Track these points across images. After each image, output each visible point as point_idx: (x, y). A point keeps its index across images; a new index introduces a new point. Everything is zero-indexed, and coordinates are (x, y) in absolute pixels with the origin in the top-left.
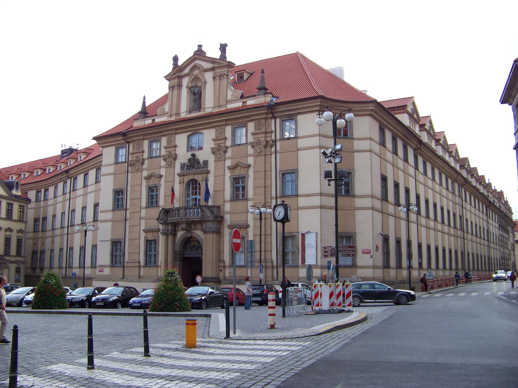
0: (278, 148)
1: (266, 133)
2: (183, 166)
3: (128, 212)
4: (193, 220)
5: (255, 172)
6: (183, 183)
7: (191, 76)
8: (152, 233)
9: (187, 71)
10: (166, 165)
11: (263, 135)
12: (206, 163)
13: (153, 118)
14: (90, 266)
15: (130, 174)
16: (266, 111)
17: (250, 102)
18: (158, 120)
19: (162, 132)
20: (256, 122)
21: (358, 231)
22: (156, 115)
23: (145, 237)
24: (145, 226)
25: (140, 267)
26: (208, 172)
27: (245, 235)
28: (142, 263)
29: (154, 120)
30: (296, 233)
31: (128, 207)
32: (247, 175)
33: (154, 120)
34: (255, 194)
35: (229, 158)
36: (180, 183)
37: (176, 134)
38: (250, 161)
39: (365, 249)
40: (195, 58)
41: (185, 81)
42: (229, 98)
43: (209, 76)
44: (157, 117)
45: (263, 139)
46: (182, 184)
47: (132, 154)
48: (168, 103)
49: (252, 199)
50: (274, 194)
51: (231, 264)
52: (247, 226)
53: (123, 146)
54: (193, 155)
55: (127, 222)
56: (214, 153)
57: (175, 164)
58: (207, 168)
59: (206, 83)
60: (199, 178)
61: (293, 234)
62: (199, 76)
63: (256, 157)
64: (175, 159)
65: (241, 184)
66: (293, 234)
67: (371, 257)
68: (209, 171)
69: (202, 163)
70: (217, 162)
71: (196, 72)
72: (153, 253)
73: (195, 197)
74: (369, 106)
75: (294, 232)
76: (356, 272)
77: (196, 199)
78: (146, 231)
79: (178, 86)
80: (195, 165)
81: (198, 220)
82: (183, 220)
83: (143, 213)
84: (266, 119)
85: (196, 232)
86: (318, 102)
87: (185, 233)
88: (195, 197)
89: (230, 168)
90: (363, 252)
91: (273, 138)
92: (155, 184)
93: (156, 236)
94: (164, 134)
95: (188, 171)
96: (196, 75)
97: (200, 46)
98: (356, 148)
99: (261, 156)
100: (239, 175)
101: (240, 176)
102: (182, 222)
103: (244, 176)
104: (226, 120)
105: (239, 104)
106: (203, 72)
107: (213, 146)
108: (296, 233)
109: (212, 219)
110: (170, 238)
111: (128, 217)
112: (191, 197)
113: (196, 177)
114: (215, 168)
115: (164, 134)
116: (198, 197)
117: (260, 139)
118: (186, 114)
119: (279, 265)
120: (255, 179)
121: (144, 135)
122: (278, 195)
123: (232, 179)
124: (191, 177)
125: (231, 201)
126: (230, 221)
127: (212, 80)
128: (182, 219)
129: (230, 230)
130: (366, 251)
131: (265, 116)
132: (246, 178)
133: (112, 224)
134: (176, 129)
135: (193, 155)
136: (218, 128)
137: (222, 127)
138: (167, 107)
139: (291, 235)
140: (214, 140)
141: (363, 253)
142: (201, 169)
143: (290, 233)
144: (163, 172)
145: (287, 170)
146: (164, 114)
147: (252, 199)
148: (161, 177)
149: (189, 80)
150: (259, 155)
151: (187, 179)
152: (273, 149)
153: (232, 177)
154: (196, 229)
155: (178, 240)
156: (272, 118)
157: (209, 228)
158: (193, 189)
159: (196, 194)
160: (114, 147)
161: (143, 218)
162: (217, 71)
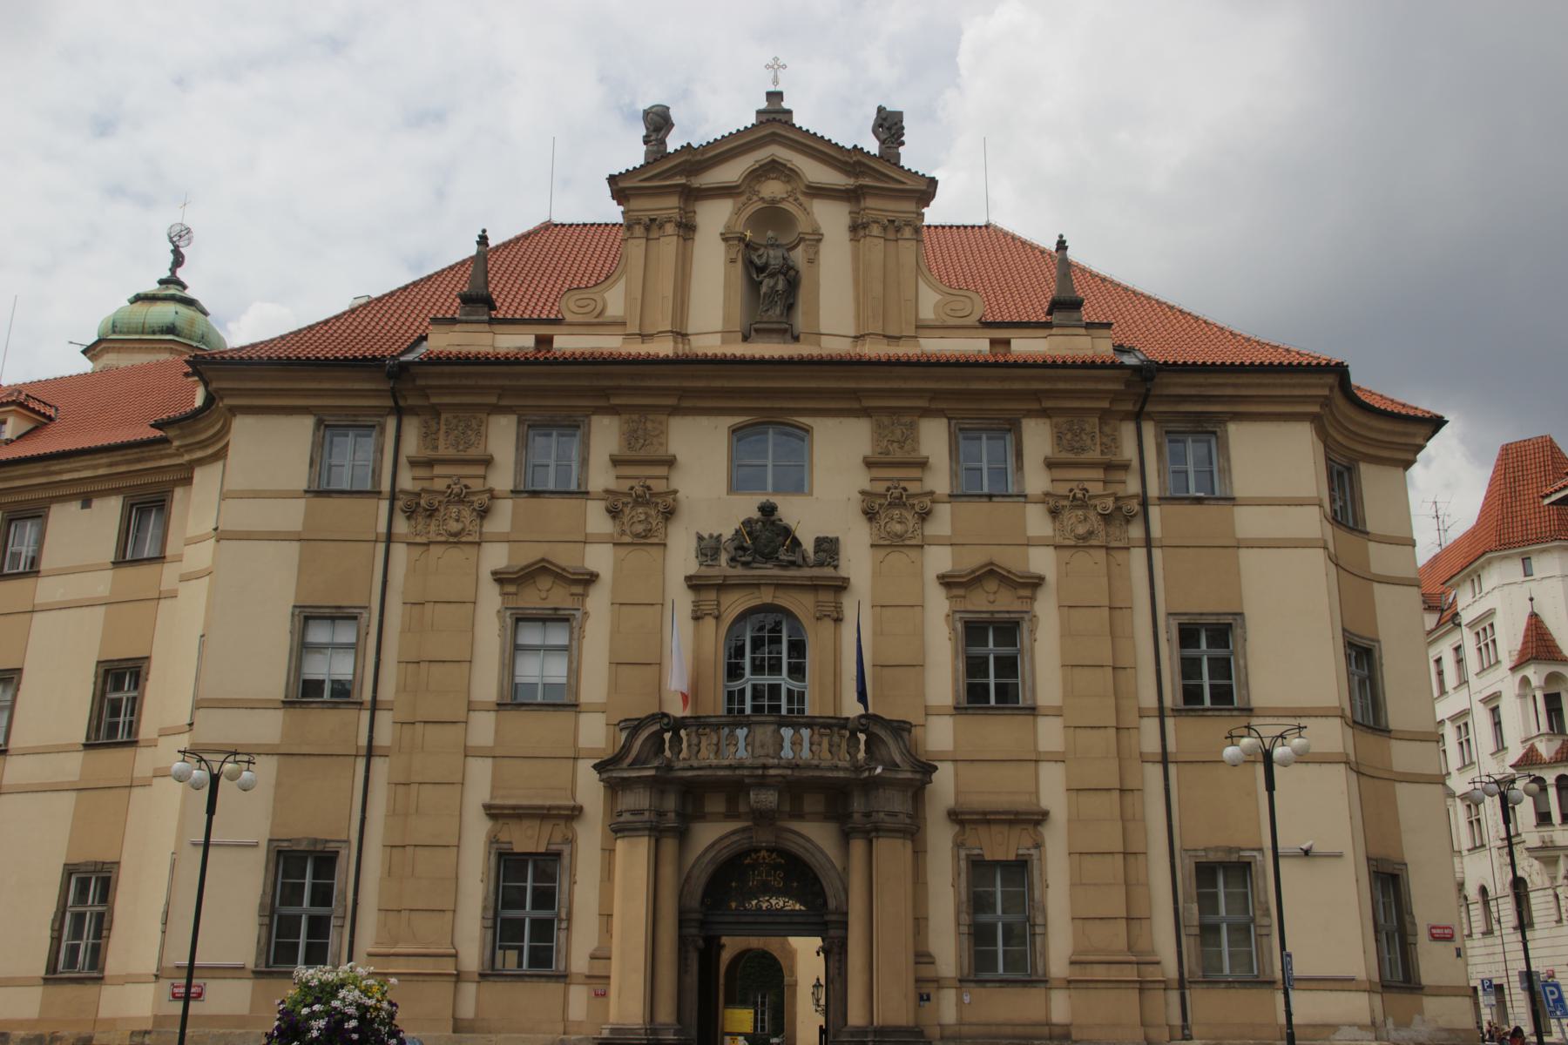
0: (1156, 531)
1: (1109, 467)
2: (708, 549)
3: (384, 718)
4: (817, 773)
5: (1067, 607)
6: (717, 618)
7: (743, 199)
8: (536, 823)
9: (730, 173)
10: (623, 533)
11: (1099, 474)
12: (828, 548)
13: (544, 330)
14: (42, 973)
15: (400, 552)
16: (1120, 387)
17: (1025, 346)
18: (566, 343)
19: (605, 393)
20: (1061, 420)
21: (1408, 858)
22: (557, 322)
23: (493, 840)
24: (494, 788)
25: (458, 977)
26: (841, 586)
27: (1033, 851)
28: (472, 956)
29: (544, 342)
30: (1253, 850)
31: (387, 692)
32: (1026, 617)
33: (544, 342)
34: (1068, 690)
35: (939, 542)
36: (697, 618)
37: (675, 411)
38: (1042, 562)
39: (1434, 923)
40: (774, 134)
41: (714, 217)
42: (927, 313)
43: (831, 219)
44: (564, 329)
45: (1096, 488)
46: (709, 623)
47: (414, 463)
48: (623, 281)
49: (1058, 712)
50: (1149, 699)
51: (966, 971)
52: (1038, 818)
53: (369, 421)
54: (768, 510)
55: (379, 765)
56: (870, 515)
57: (666, 535)
58: (836, 567)
59: (819, 241)
60: (801, 604)
61: (1242, 853)
62: (784, 205)
63: (1067, 554)
64: (669, 514)
65: (991, 649)
66: (1242, 853)
67: (1459, 955)
68: (847, 580)
69: (808, 545)
70: (889, 550)
71: (773, 189)
72: (528, 913)
73: (766, 679)
74: (1414, 435)
75: (1243, 846)
76: (1420, 1011)
77: (775, 690)
78: (494, 812)
79: (679, 225)
80: (782, 550)
81: (842, 774)
82: (772, 772)
83: (483, 728)
84: (1105, 416)
85: (796, 826)
86: (1323, 386)
87: (744, 830)
88: (766, 679)
89: (948, 582)
90: (1432, 935)
91: (1133, 486)
92: (556, 609)
93: (558, 837)
94: (615, 401)
95: (740, 571)
96: (773, 201)
97: (776, 96)
98: (1376, 568)
99: (1092, 551)
100: (992, 613)
101: (997, 615)
102: (762, 783)
103: (1012, 615)
104: (935, 395)
105: (977, 345)
106: (805, 194)
107: (867, 486)
108: (1255, 853)
109: (909, 775)
110: (669, 846)
111: (384, 737)
112: (749, 680)
113: (786, 600)
114: (877, 574)
115: (615, 401)
116: (784, 681)
117: (1087, 485)
118: (724, 342)
119: (1186, 975)
120: (1067, 633)
121: (503, 392)
122: (1168, 702)
123: (959, 626)
124: (766, 597)
125: (958, 710)
126: (957, 793)
127: (845, 235)
128: (765, 767)
129: (957, 828)
130: (1438, 931)
131: (1106, 405)
132: (1025, 627)
133: (279, 771)
134: (684, 393)
135: (768, 510)
136: (886, 420)
137: (907, 419)
138: (615, 301)
139: (1234, 858)
140: (869, 464)
141: (1434, 938)
142: (806, 572)
143: (1230, 850)
144: (599, 559)
145: (1202, 614)
146: (599, 324)
147: (1058, 712)
148: (590, 579)
149: (738, 212)
150: (1083, 543)
151: (735, 604)
152: (1136, 531)
153: (958, 616)
154: (799, 816)
155: (699, 858)
156: (1126, 416)
157: (890, 814)
158: (753, 651)
159: (775, 668)
160: (308, 422)
161: (481, 753)
162: (870, 203)
